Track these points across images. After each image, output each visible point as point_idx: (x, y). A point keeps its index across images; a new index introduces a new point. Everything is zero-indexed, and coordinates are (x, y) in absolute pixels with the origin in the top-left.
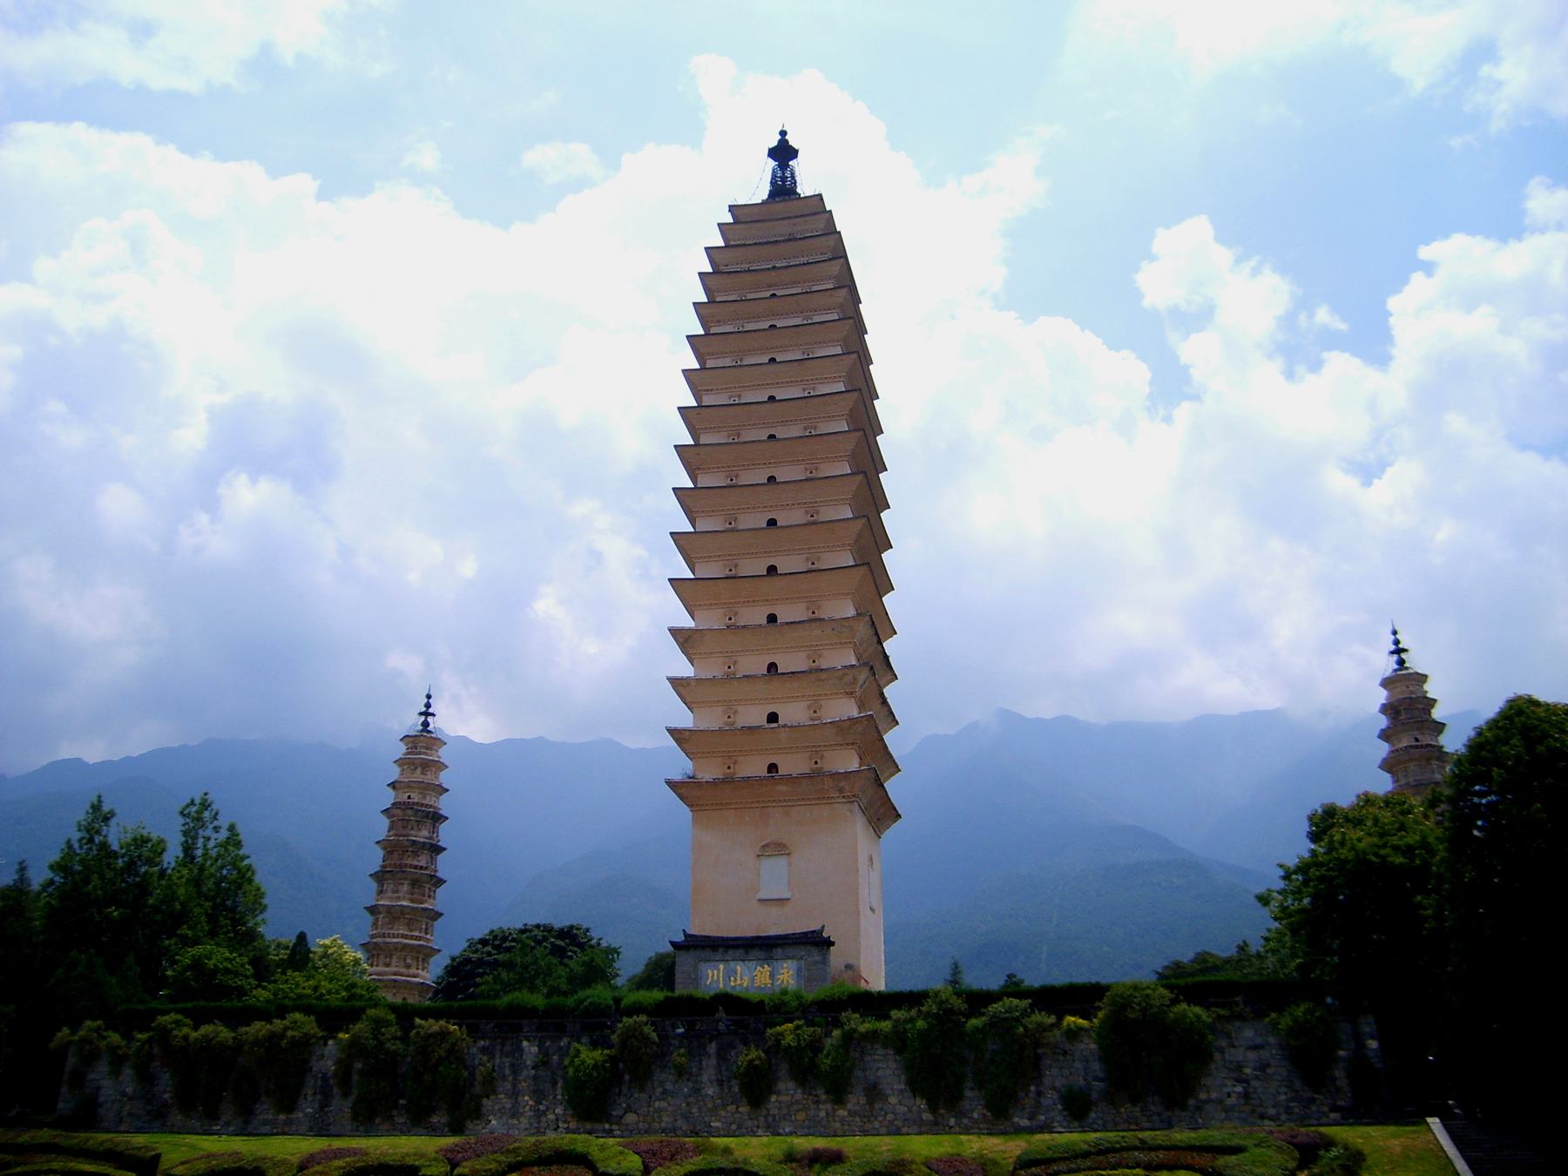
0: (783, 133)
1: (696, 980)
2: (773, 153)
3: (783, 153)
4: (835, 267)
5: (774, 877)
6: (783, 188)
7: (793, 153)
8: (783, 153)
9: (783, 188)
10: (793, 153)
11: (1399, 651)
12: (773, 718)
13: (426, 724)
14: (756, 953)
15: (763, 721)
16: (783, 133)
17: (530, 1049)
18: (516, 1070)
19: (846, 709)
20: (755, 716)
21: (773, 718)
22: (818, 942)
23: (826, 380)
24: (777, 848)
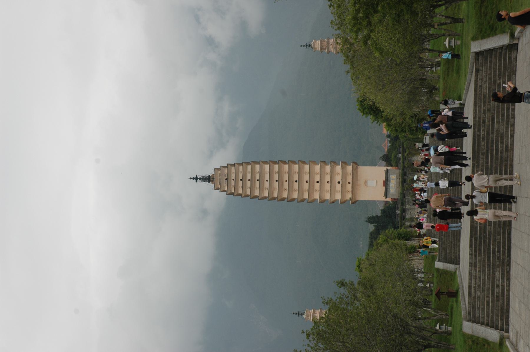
0: (191, 178)
1: (392, 195)
2: (196, 181)
3: (196, 179)
4: (236, 165)
5: (372, 183)
6: (207, 179)
7: (197, 176)
8: (196, 179)
9: (207, 179)
10: (197, 176)
11: (306, 46)
12: (339, 183)
13: (302, 314)
14: (388, 183)
15: (340, 184)
16: (191, 178)
17: (407, 207)
18: (411, 209)
19: (339, 168)
20: (338, 187)
21: (339, 183)
22: (387, 172)
23: (264, 169)
24: (366, 182)
